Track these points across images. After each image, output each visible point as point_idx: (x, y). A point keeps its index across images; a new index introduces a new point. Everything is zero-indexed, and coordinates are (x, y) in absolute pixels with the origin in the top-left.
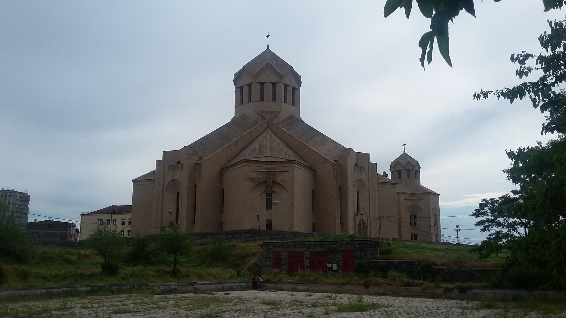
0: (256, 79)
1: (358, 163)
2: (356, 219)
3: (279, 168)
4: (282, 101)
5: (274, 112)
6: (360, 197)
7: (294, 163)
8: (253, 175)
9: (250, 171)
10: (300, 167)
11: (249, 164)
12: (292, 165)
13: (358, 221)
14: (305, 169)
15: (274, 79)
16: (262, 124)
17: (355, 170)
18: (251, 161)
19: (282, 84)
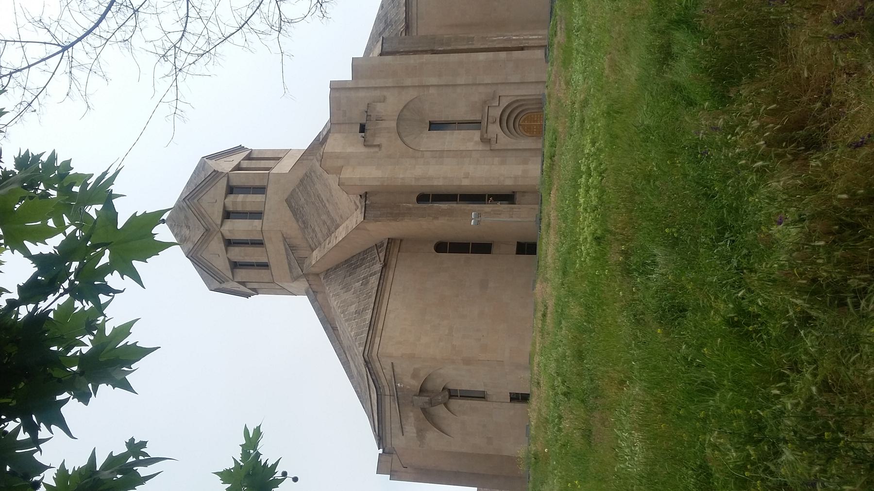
0: (228, 279)
1: (357, 123)
2: (497, 147)
3: (388, 377)
4: (260, 230)
5: (286, 249)
6: (443, 118)
7: (372, 356)
8: (411, 429)
9: (403, 435)
10: (380, 326)
11: (388, 436)
12: (375, 357)
13: (504, 140)
14: (386, 295)
15: (216, 245)
16: (314, 292)
17: (375, 144)
18: (381, 432)
19: (222, 228)
